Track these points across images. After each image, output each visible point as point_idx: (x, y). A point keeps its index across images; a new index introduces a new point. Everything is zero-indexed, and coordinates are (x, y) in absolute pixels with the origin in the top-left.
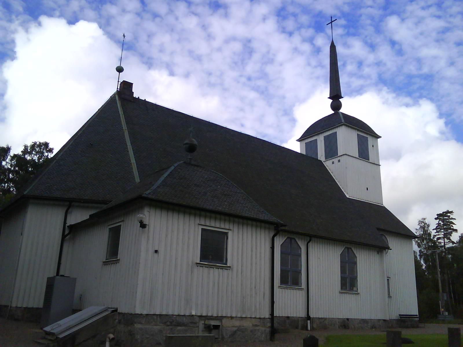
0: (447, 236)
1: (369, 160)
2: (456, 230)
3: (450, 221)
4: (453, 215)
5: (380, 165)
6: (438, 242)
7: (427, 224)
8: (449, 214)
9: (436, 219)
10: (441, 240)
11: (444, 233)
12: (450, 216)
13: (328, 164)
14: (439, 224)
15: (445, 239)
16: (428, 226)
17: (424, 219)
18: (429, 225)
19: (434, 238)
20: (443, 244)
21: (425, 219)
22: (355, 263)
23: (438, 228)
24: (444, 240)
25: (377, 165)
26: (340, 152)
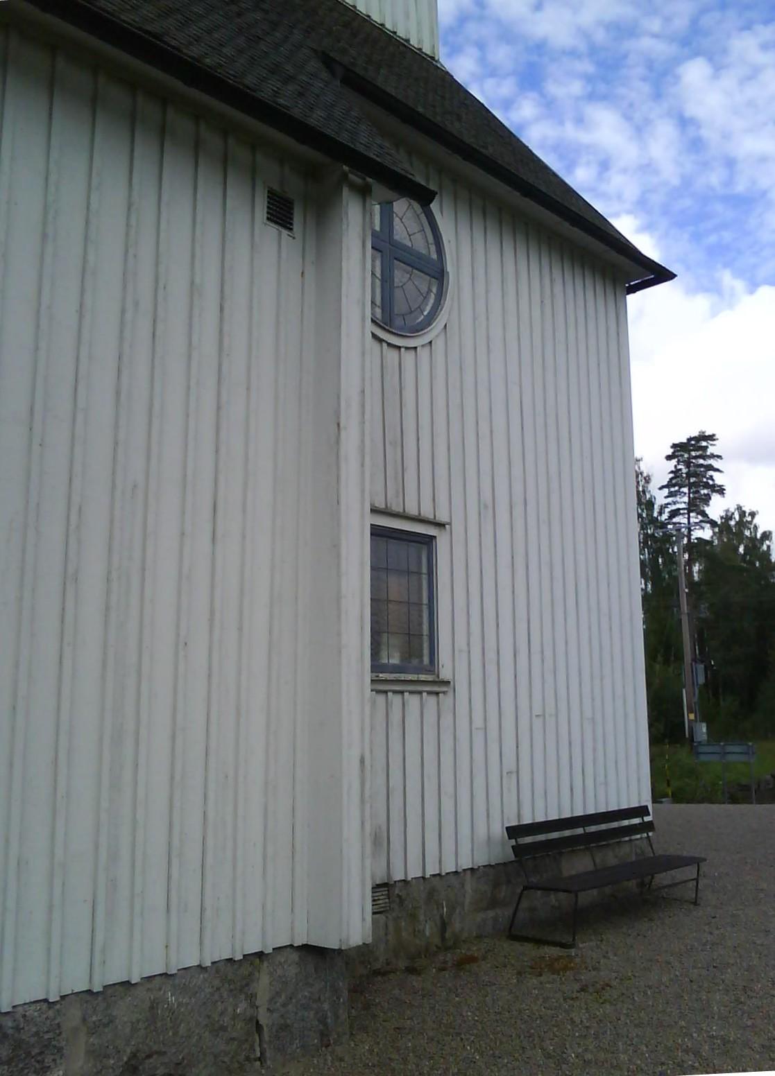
0: (697, 505)
2: (721, 490)
4: (714, 445)
6: (675, 524)
7: (645, 475)
8: (704, 444)
9: (669, 458)
10: (681, 517)
11: (689, 497)
14: (676, 472)
16: (648, 480)
18: (649, 479)
19: (660, 513)
21: (639, 460)
23: (675, 482)
24: (689, 519)
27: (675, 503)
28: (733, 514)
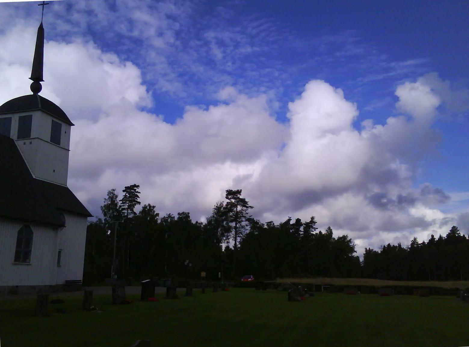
0: (131, 207)
1: (59, 145)
2: (139, 203)
3: (136, 194)
5: (70, 150)
6: (123, 212)
7: (116, 195)
8: (135, 188)
9: (124, 191)
11: (129, 204)
12: (136, 189)
13: (20, 144)
14: (125, 196)
15: (129, 210)
16: (117, 197)
17: (114, 190)
20: (126, 214)
22: (31, 239)
23: (124, 200)
25: (66, 149)
26: (33, 135)
27: (124, 206)
28: (147, 206)
